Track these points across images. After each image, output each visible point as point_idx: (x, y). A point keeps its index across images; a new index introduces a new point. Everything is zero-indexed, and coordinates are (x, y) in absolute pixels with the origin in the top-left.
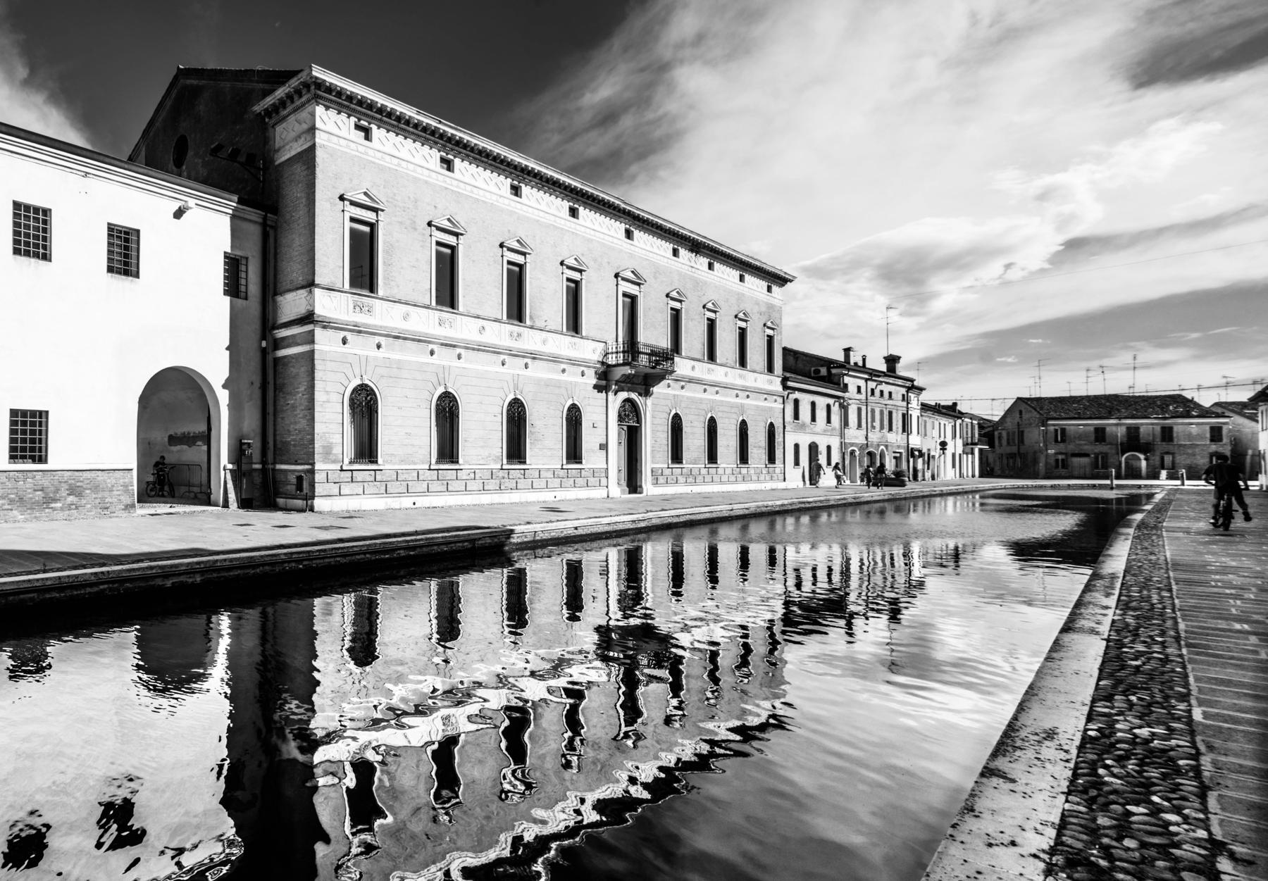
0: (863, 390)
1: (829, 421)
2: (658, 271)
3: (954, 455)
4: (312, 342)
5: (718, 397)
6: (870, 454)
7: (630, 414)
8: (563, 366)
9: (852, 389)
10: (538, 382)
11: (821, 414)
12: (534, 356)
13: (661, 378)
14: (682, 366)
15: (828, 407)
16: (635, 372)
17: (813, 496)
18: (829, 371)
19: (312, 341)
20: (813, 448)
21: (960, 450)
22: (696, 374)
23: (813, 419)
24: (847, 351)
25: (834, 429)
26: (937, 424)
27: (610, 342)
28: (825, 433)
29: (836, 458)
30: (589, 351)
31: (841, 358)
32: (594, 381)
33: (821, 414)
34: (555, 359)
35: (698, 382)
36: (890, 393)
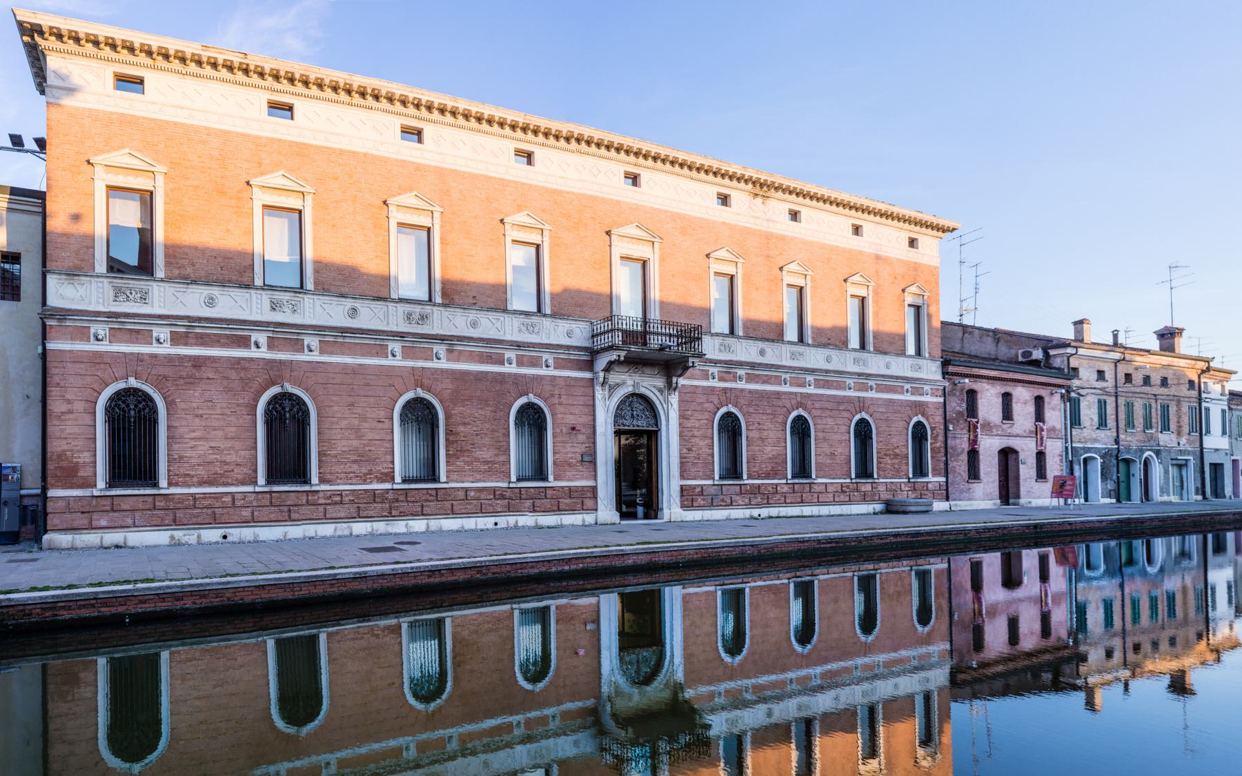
0: (1109, 375)
1: (1039, 416)
17: (1008, 518)
18: (1047, 355)
20: (1007, 456)
23: (1007, 414)
24: (1079, 324)
29: (1055, 467)
31: (1068, 334)
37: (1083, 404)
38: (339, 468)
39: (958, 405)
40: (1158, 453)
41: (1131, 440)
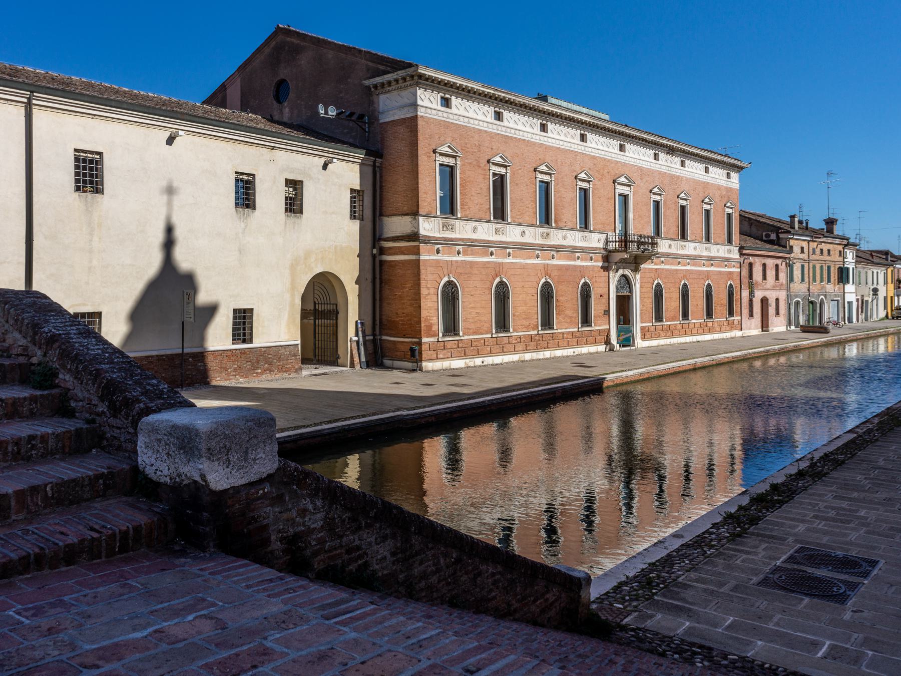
0: (806, 250)
1: (777, 278)
2: (644, 172)
3: (885, 298)
4: (418, 254)
5: (689, 268)
6: (812, 302)
7: (626, 281)
8: (578, 254)
9: (797, 250)
10: (560, 268)
11: (771, 273)
12: (558, 248)
13: (649, 258)
14: (663, 246)
15: (777, 266)
16: (629, 253)
19: (418, 253)
21: (891, 293)
22: (673, 251)
23: (765, 278)
25: (782, 284)
26: (870, 273)
27: (610, 233)
28: (774, 288)
30: (596, 241)
32: (600, 264)
33: (771, 273)
34: (573, 249)
35: (675, 256)
36: (829, 251)
37: (795, 268)
38: (519, 323)
39: (745, 272)
40: (825, 296)
41: (815, 288)
